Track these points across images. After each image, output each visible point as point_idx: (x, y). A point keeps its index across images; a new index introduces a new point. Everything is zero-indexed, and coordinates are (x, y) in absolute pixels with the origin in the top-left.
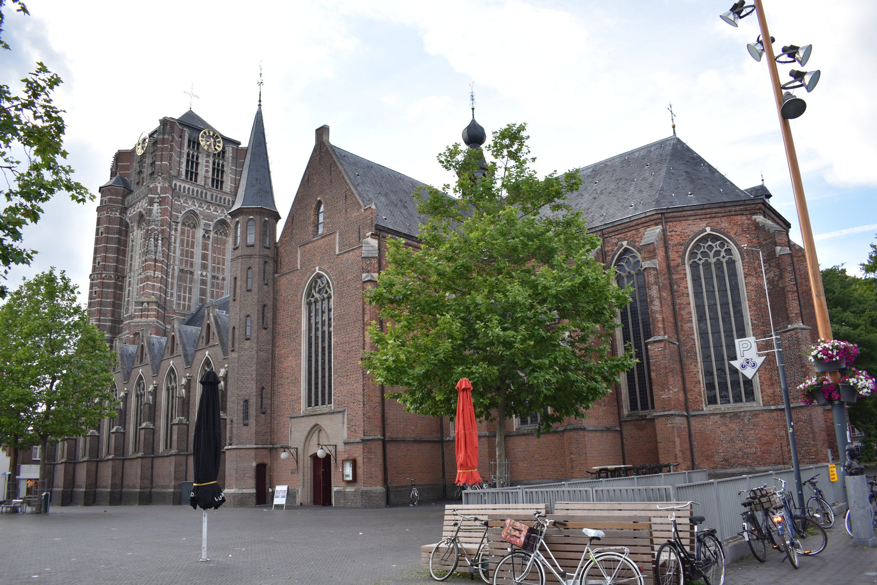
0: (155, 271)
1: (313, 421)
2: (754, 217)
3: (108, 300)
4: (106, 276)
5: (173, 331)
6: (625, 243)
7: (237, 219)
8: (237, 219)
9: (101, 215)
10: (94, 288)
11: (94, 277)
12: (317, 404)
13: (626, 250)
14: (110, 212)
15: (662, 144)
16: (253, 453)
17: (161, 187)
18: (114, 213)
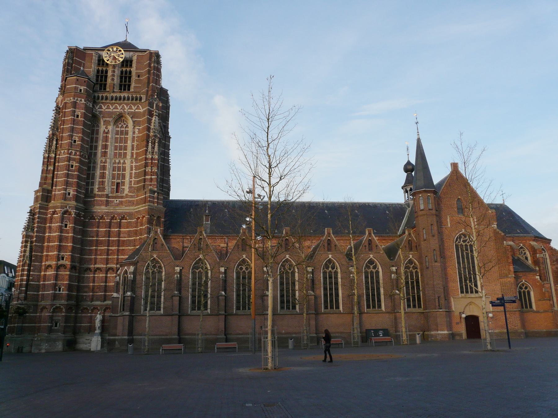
1: (470, 300)
2: (530, 242)
3: (83, 176)
4: (83, 155)
5: (329, 237)
6: (521, 245)
7: (429, 194)
8: (429, 194)
9: (77, 100)
10: (71, 162)
11: (71, 152)
12: (467, 292)
13: (522, 248)
14: (87, 101)
15: (501, 205)
16: (444, 313)
17: (156, 104)
18: (89, 103)
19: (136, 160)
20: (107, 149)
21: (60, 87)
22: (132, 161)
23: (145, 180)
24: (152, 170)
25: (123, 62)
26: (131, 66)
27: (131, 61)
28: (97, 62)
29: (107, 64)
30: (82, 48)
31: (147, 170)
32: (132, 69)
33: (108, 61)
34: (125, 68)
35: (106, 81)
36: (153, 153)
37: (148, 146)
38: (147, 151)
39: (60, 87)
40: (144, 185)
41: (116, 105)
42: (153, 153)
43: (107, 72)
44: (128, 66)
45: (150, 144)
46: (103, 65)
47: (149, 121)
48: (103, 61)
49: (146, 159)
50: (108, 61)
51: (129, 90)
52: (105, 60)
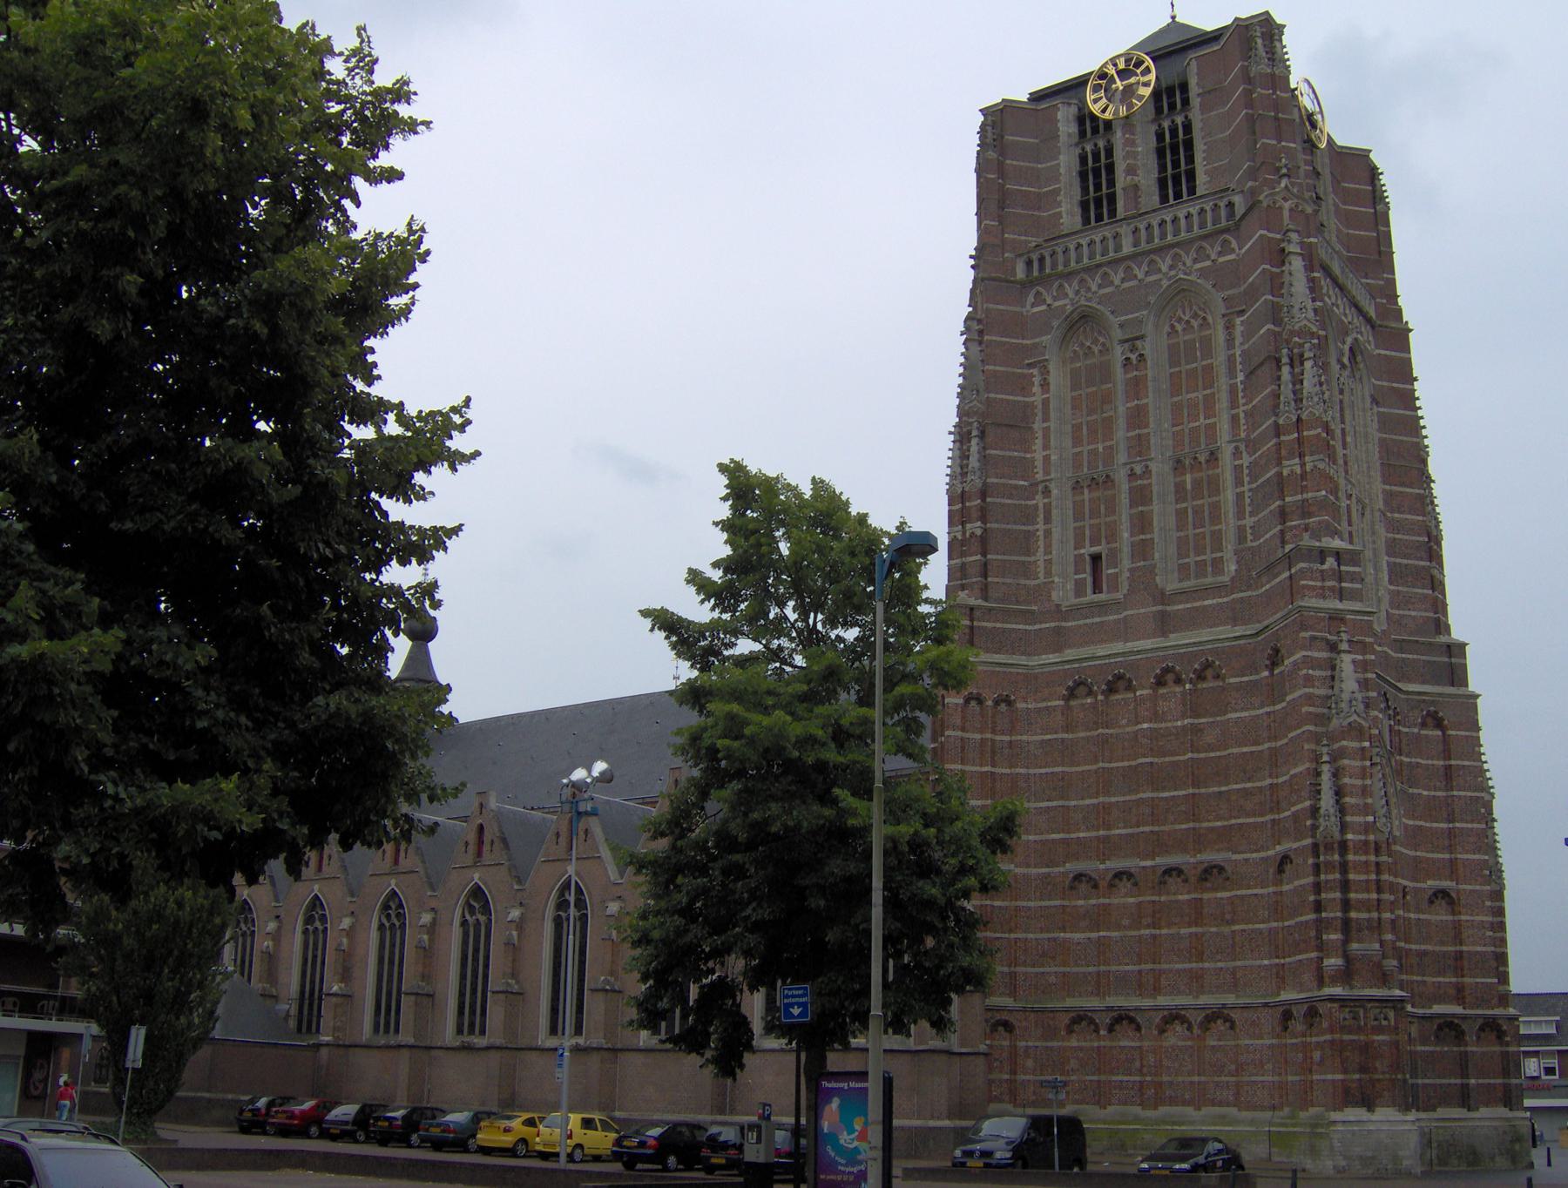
0: (1301, 456)
19: (1252, 446)
20: (1147, 426)
21: (974, 253)
22: (1237, 448)
23: (1283, 515)
24: (1303, 465)
25: (1156, 94)
26: (1186, 102)
27: (1184, 87)
28: (1074, 129)
29: (1108, 124)
30: (1024, 98)
31: (1285, 473)
32: (1191, 116)
33: (1104, 111)
34: (1168, 116)
35: (1111, 183)
36: (1298, 400)
37: (1279, 378)
38: (1279, 396)
39: (974, 253)
40: (1282, 532)
41: (1153, 256)
42: (1298, 400)
43: (1109, 152)
44: (1175, 107)
45: (1286, 370)
46: (1095, 131)
47: (1276, 284)
48: (1093, 117)
49: (1278, 430)
50: (1104, 111)
51: (1192, 190)
52: (1096, 109)
